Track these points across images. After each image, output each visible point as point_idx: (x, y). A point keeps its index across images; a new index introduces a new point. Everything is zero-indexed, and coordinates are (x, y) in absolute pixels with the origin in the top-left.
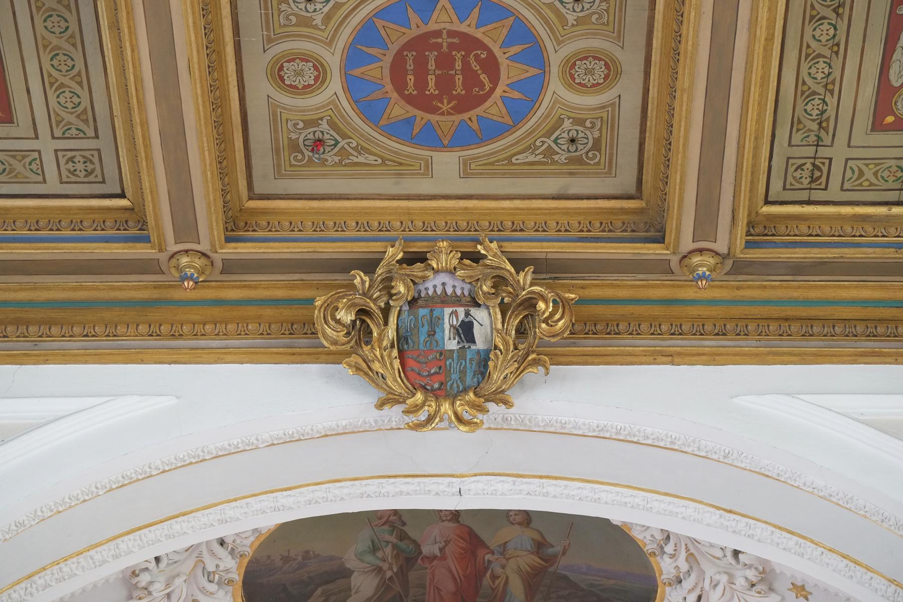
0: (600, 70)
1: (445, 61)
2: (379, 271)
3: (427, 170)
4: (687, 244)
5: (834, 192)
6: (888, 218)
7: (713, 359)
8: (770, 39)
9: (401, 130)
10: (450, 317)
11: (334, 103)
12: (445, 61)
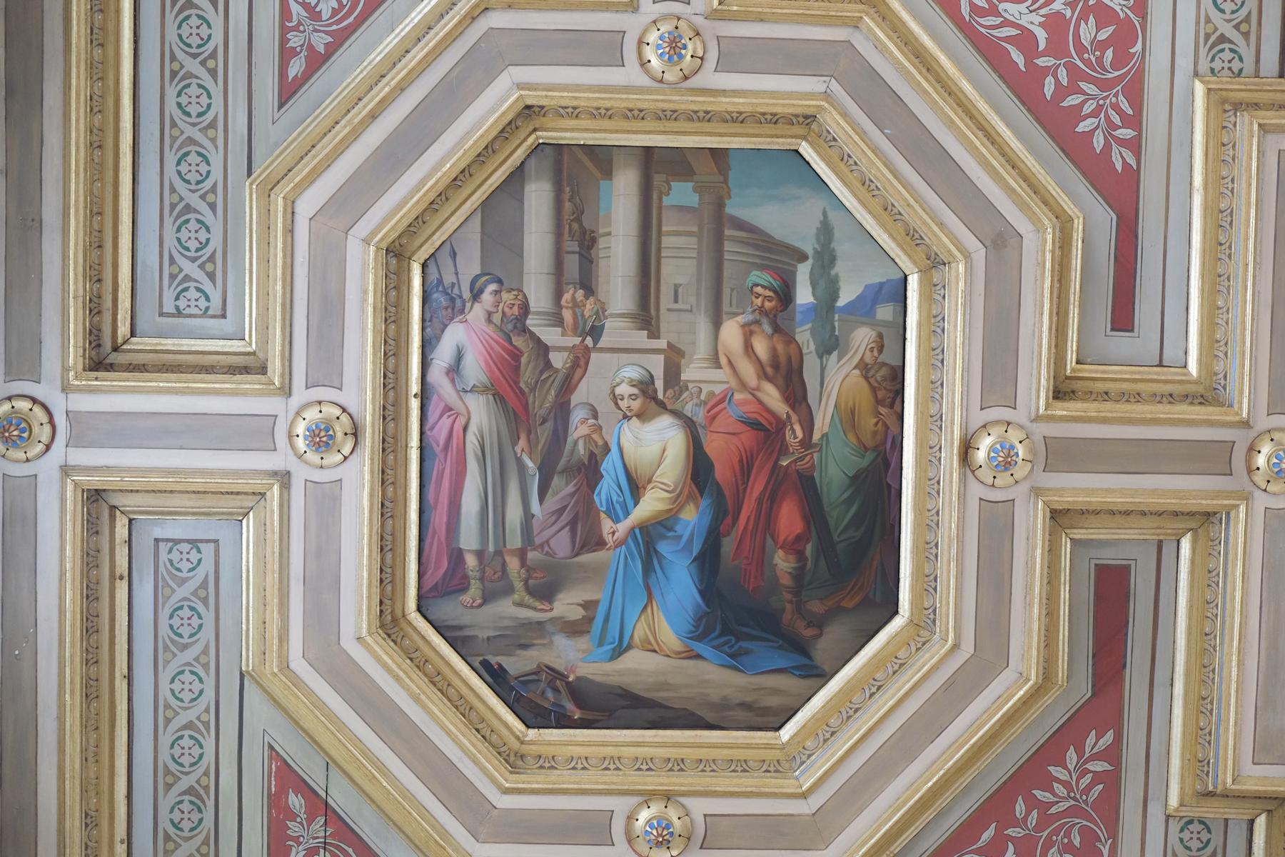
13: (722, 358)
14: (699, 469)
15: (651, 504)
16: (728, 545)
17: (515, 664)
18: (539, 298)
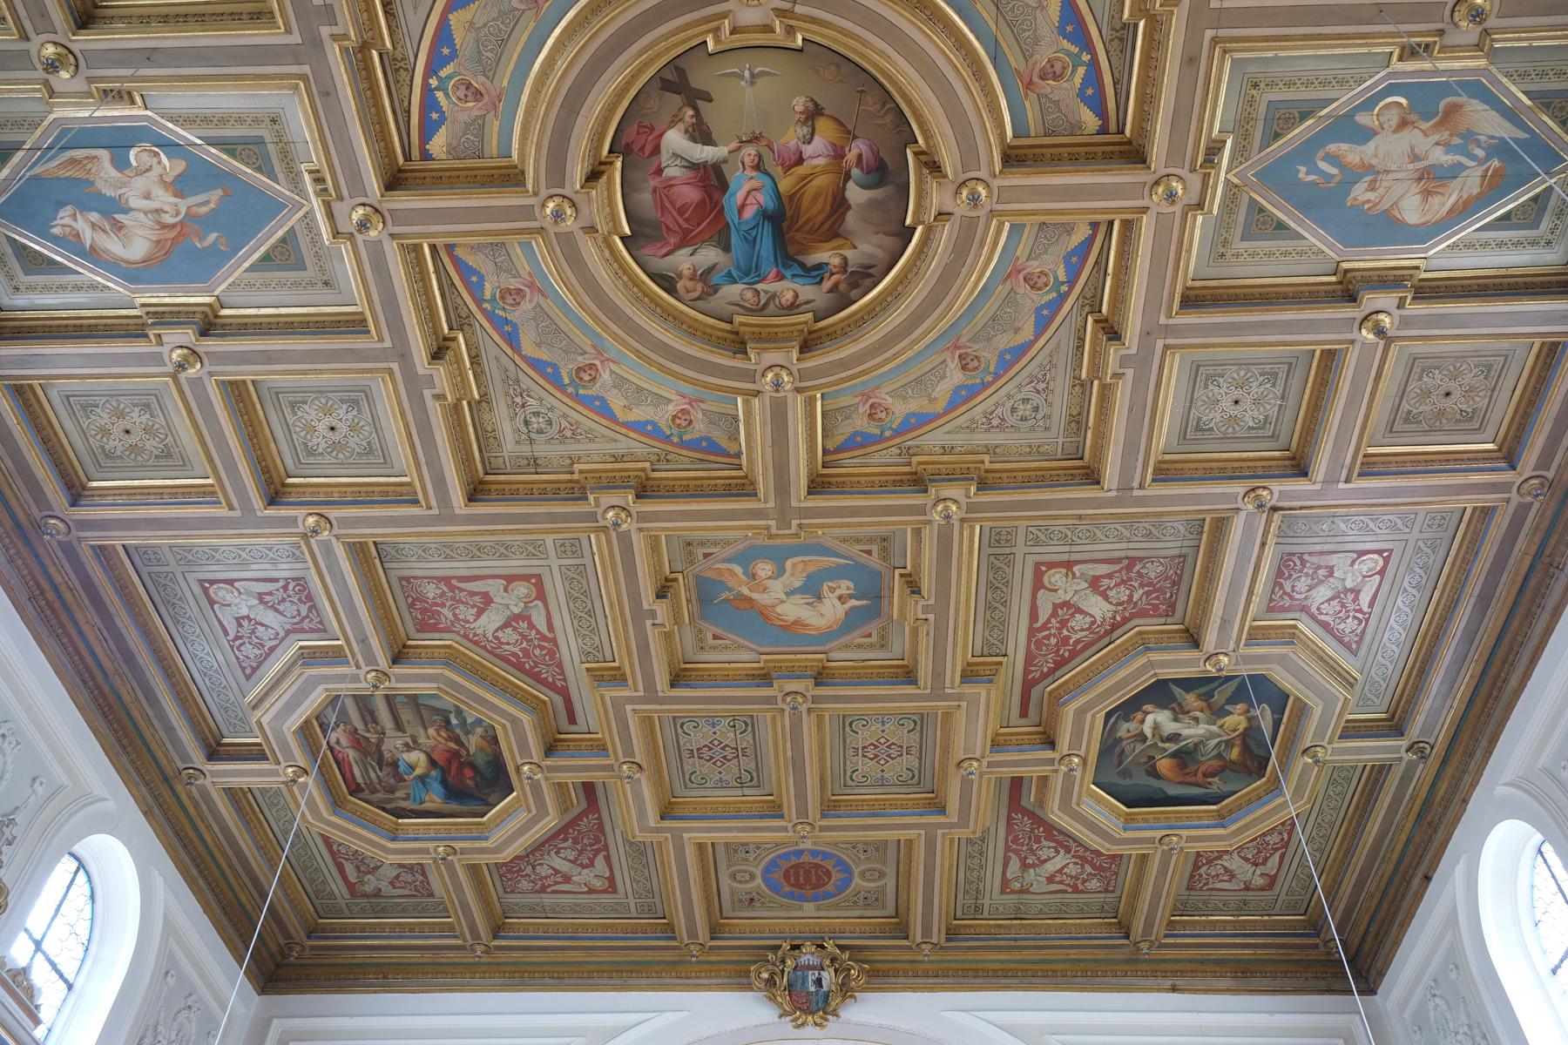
0: (876, 875)
1: (807, 872)
2: (780, 953)
3: (801, 908)
4: (919, 940)
5: (986, 915)
6: (1010, 927)
7: (932, 990)
8: (951, 867)
9: (791, 896)
10: (811, 976)
11: (758, 886)
12: (807, 872)
13: (431, 737)
14: (433, 763)
15: (418, 771)
16: (450, 779)
17: (388, 806)
18: (360, 726)
